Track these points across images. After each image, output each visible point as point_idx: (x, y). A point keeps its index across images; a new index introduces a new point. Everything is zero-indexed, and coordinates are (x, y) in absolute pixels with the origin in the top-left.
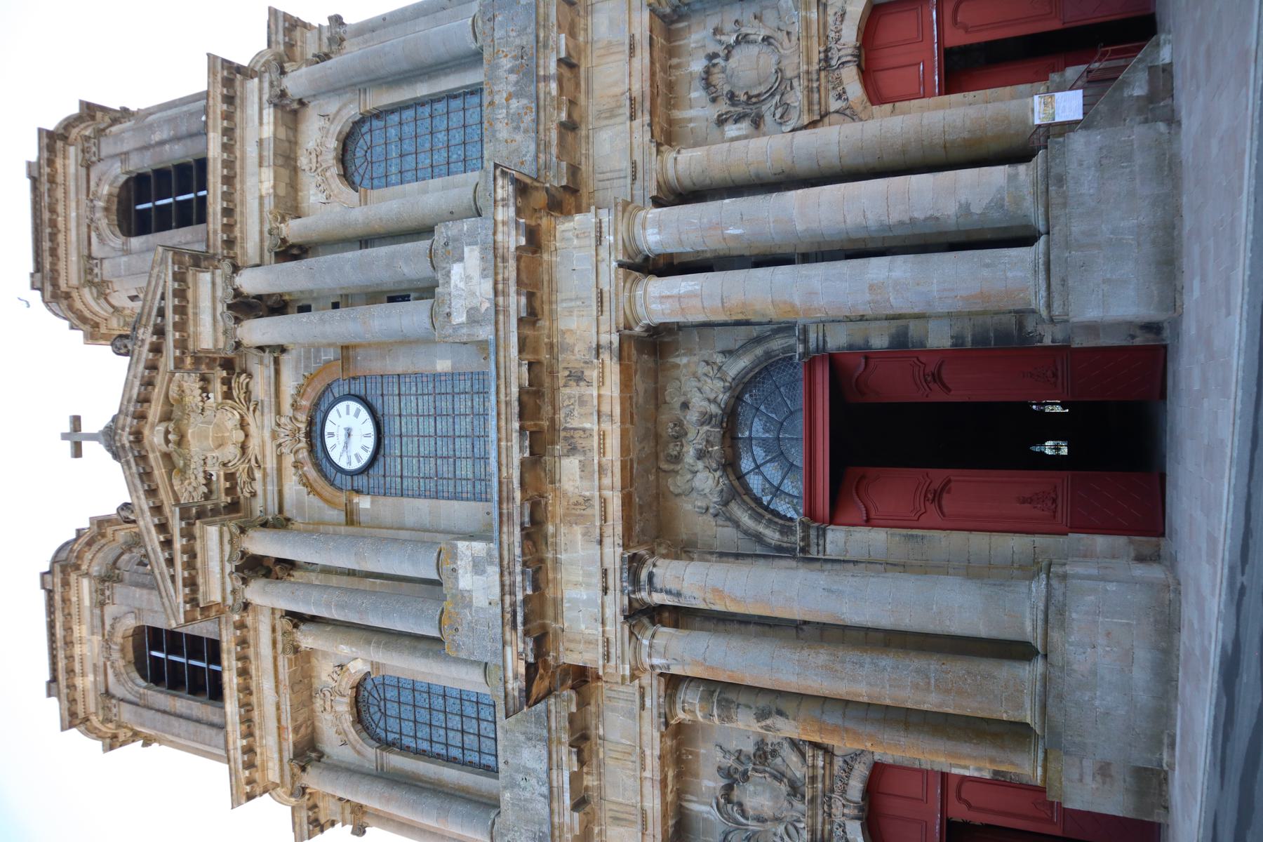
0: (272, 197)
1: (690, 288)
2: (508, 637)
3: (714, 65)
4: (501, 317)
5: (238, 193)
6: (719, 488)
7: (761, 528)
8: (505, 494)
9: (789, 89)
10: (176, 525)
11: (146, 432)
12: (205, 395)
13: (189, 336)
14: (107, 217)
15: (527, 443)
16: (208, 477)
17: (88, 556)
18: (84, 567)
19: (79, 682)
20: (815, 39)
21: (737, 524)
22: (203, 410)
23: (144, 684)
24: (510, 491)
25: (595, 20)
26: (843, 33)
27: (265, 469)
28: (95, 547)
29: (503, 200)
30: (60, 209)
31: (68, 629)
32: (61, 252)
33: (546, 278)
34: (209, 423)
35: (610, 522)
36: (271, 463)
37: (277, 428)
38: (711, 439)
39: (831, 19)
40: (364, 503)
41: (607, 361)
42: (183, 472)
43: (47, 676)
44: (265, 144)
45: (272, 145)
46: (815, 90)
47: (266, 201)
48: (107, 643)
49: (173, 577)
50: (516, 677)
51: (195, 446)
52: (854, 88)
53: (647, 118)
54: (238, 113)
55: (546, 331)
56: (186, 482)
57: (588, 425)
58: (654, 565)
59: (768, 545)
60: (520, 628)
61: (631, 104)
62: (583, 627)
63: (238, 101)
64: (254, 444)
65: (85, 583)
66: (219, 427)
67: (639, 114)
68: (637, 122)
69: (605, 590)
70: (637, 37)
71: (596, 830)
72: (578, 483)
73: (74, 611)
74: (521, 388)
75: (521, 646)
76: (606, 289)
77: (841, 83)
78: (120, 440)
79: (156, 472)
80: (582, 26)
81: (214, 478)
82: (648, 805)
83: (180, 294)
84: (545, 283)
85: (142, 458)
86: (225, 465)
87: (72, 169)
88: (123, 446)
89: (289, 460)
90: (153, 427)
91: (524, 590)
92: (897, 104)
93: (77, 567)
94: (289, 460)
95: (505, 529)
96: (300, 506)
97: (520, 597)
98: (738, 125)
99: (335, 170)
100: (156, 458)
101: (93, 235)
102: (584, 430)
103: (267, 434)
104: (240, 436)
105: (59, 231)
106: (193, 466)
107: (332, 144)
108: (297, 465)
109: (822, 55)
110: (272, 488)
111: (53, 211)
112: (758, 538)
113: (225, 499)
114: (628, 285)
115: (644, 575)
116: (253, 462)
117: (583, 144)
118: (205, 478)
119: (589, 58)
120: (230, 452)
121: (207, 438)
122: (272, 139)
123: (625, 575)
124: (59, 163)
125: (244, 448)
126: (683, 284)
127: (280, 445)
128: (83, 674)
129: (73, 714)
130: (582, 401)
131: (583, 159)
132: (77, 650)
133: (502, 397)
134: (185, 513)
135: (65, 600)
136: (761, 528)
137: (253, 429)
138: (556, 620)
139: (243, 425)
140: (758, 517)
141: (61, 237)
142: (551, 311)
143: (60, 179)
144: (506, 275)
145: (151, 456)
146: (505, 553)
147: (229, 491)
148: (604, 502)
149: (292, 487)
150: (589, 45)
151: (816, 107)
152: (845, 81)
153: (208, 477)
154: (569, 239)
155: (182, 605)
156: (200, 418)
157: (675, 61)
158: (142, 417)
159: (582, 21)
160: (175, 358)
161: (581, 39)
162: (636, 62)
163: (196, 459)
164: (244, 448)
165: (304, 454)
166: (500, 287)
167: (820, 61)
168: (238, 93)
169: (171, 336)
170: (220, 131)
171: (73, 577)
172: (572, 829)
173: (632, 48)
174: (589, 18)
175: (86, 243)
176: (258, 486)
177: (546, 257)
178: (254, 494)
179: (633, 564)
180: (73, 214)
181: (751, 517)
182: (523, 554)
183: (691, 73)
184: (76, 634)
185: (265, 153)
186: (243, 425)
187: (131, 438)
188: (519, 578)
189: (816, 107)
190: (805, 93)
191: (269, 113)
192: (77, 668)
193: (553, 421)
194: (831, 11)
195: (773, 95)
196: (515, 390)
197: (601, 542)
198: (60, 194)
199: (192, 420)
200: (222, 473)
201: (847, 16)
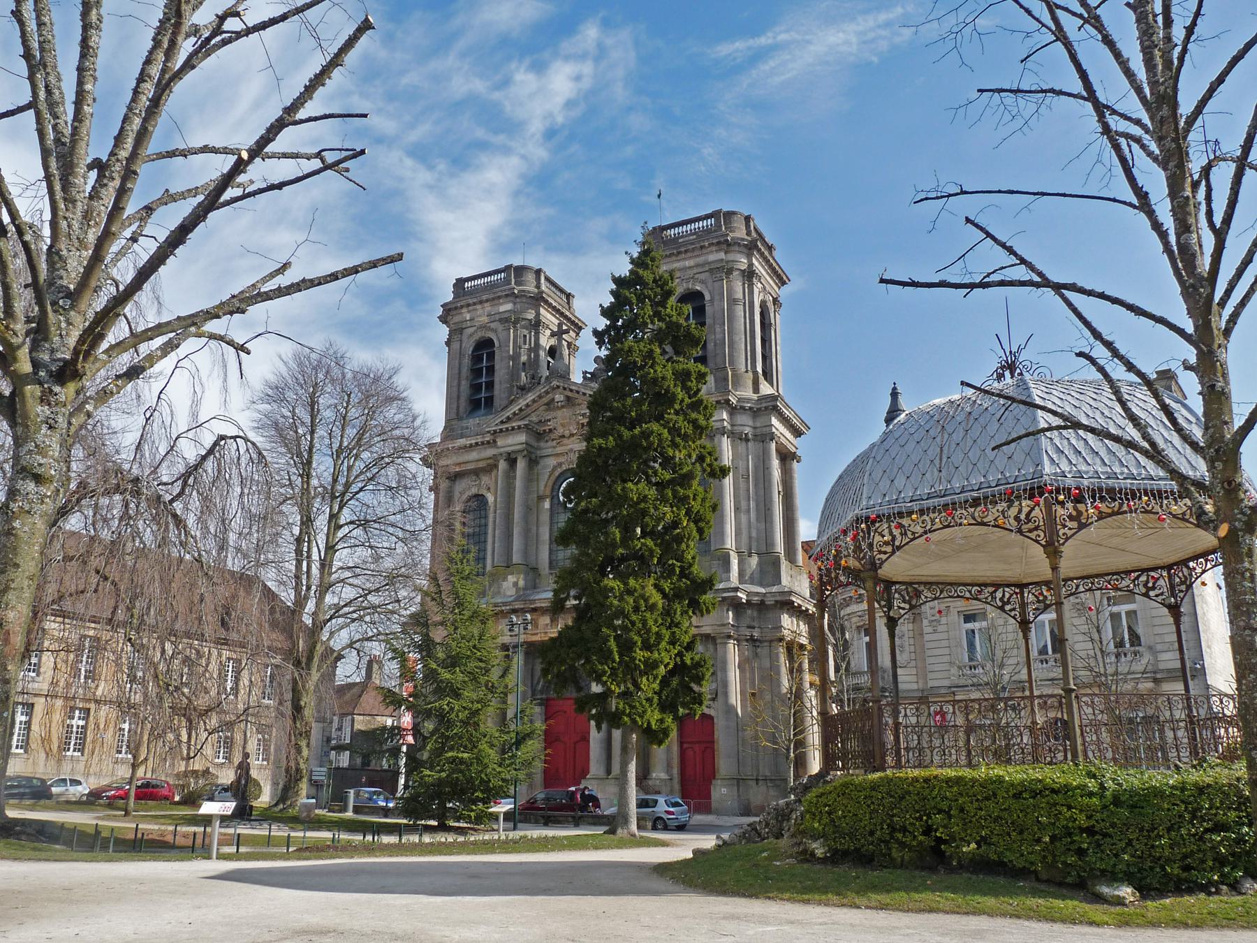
16: (549, 420)
18: (518, 300)
19: (464, 310)
30: (689, 254)
31: (487, 301)
36: (559, 450)
40: (547, 505)
42: (547, 410)
48: (483, 327)
49: (502, 422)
51: (559, 413)
64: (565, 441)
66: (569, 424)
73: (496, 302)
85: (547, 393)
89: (561, 459)
94: (561, 459)
96: (545, 467)
104: (567, 433)
108: (560, 465)
110: (550, 451)
111: (686, 251)
113: (541, 429)
120: (560, 431)
124: (714, 248)
125: (563, 436)
128: (469, 312)
129: (450, 310)
132: (478, 307)
135: (499, 297)
137: (572, 439)
139: (572, 435)
143: (704, 251)
147: (544, 431)
149: (552, 462)
153: (549, 420)
156: (571, 413)
164: (563, 436)
165: (564, 467)
176: (550, 444)
178: (547, 441)
180: (687, 263)
184: (486, 305)
186: (572, 435)
192: (471, 308)
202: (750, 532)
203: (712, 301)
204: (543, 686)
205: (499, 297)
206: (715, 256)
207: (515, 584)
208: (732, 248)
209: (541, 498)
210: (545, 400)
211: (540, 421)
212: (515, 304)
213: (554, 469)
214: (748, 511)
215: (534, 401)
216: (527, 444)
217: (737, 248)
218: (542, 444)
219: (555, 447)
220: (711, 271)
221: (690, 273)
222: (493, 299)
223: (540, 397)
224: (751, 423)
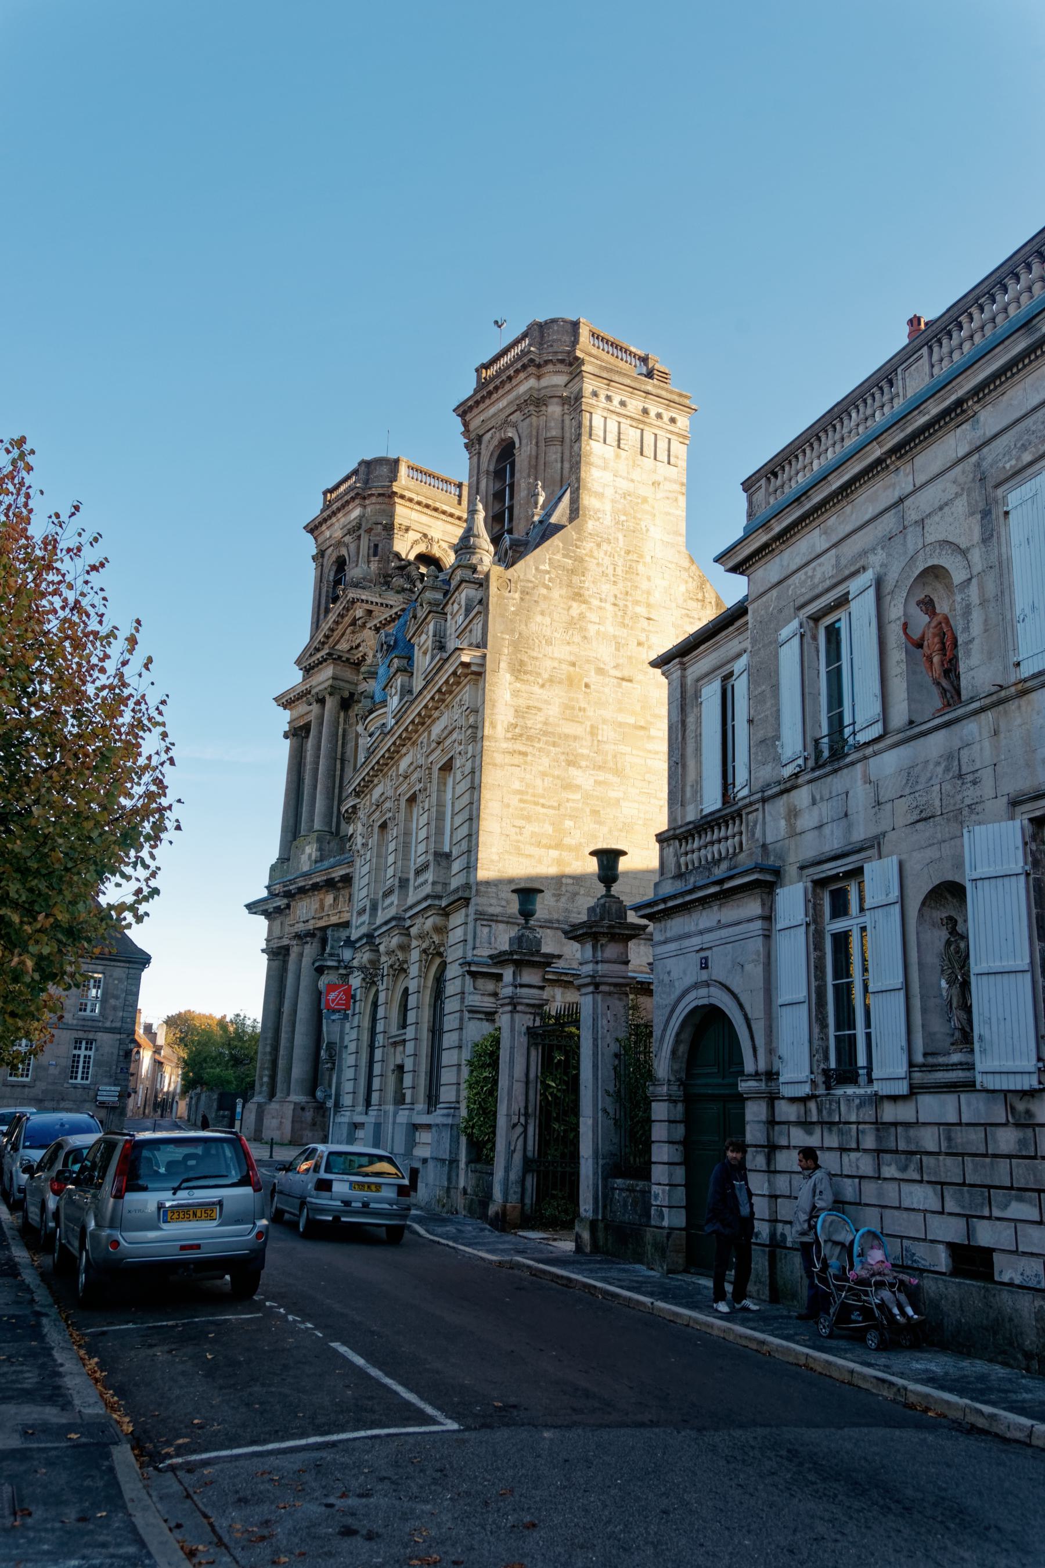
10: (323, 653)
16: (358, 646)
17: (374, 499)
18: (367, 502)
19: (324, 527)
23: (331, 578)
24: (310, 879)
28: (380, 500)
30: (501, 392)
31: (339, 510)
32: (482, 406)
42: (353, 632)
43: (330, 486)
48: (339, 543)
49: (311, 655)
65: (357, 513)
87: (522, 389)
93: (364, 498)
97: (291, 887)
101: (489, 435)
111: (496, 388)
124: (522, 375)
132: (334, 520)
135: (347, 503)
141: (488, 402)
143: (514, 382)
148: (322, 918)
153: (358, 646)
171: (357, 501)
175: (487, 428)
184: (340, 515)
192: (329, 523)
198: (508, 387)
205: (347, 503)
206: (526, 385)
208: (545, 370)
210: (347, 620)
211: (352, 648)
212: (365, 507)
215: (337, 623)
216: (333, 678)
217: (550, 367)
220: (519, 408)
221: (503, 416)
222: (343, 506)
223: (341, 616)
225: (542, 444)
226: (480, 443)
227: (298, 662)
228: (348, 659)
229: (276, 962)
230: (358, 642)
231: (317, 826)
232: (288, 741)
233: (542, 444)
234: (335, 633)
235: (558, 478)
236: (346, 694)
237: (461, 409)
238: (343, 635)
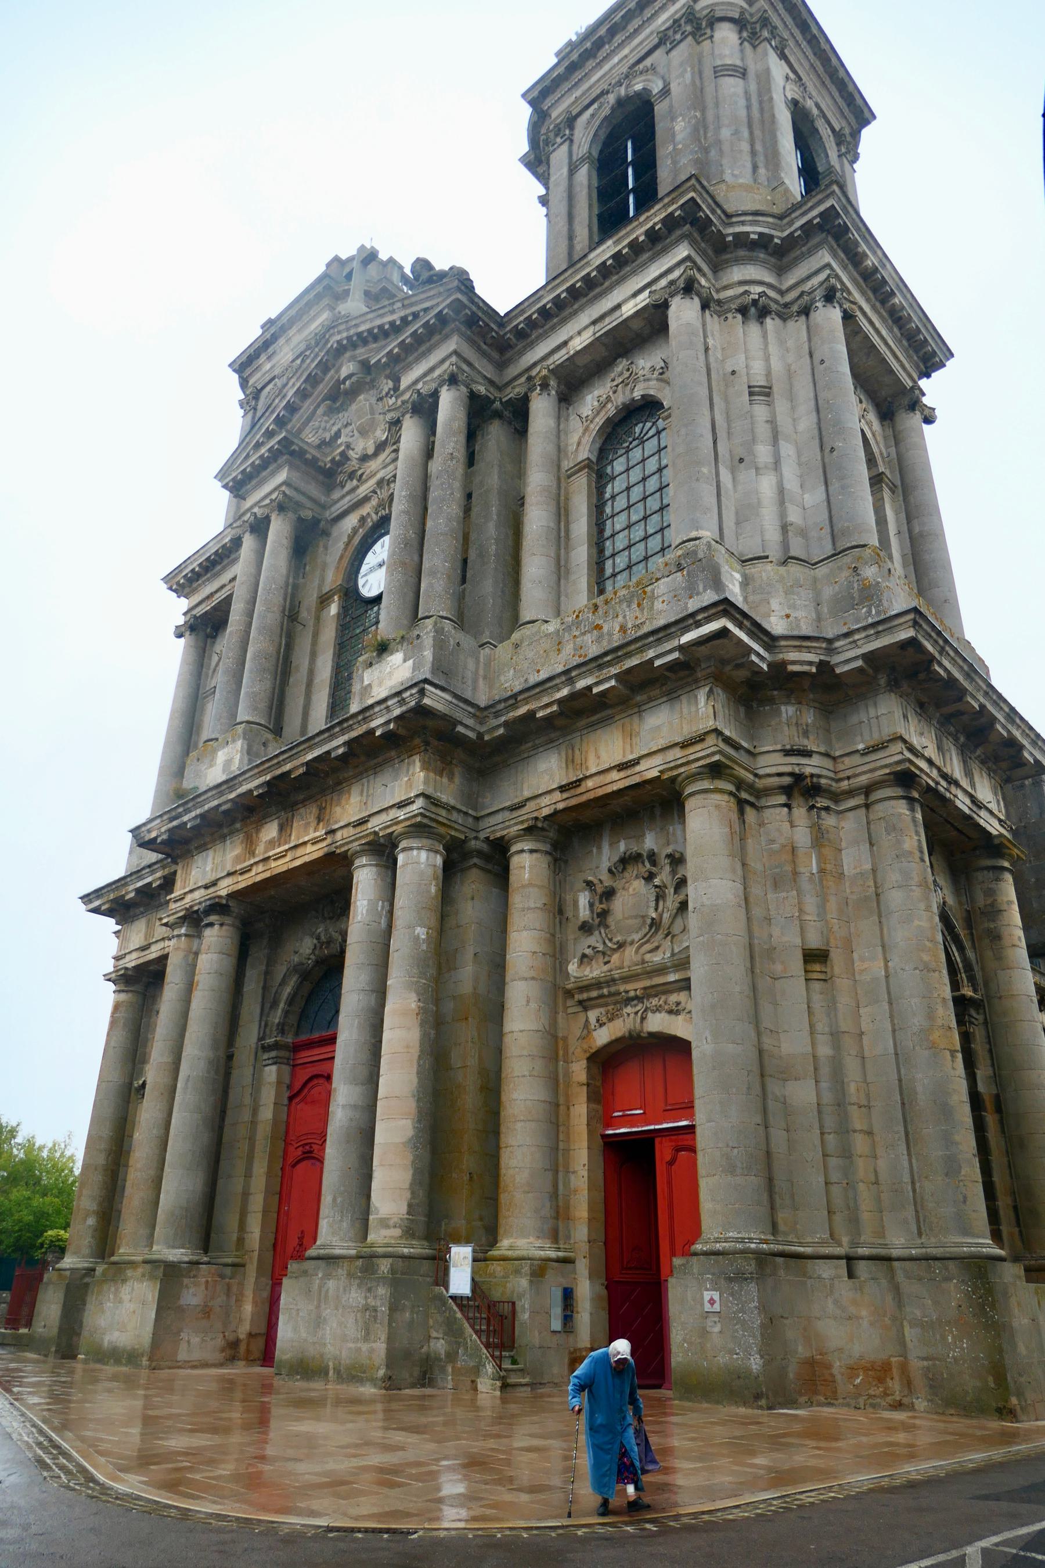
0: (566, 357)
1: (360, 910)
2: (165, 817)
3: (643, 863)
4: (326, 735)
5: (571, 310)
6: (305, 961)
7: (282, 1005)
8: (231, 784)
9: (606, 959)
11: (348, 354)
12: (392, 392)
13: (404, 360)
14: (613, 109)
15: (261, 791)
16: (338, 434)
19: (263, 358)
20: (647, 983)
21: (283, 983)
22: (381, 399)
25: (663, 706)
26: (658, 1014)
27: (357, 487)
29: (403, 699)
30: (618, 38)
33: (380, 759)
34: (372, 413)
35: (240, 878)
36: (363, 490)
37: (385, 483)
38: (332, 945)
39: (673, 998)
40: (334, 609)
41: (324, 844)
42: (331, 411)
44: (617, 313)
45: (614, 324)
46: (600, 992)
47: (563, 351)
49: (247, 456)
50: (149, 831)
52: (602, 1037)
53: (561, 806)
54: (646, 256)
55: (346, 775)
56: (326, 418)
57: (293, 838)
58: (222, 925)
59: (268, 1016)
60: (171, 825)
61: (572, 783)
62: (193, 873)
63: (659, 247)
67: (565, 795)
68: (557, 796)
69: (206, 887)
70: (638, 768)
71: (142, 909)
72: (264, 840)
74: (289, 772)
75: (163, 830)
76: (370, 825)
77: (610, 1020)
78: (330, 336)
79: (321, 386)
80: (652, 694)
81: (339, 441)
82: (154, 948)
83: (430, 331)
84: (375, 761)
86: (348, 446)
88: (327, 341)
90: (353, 358)
91: (190, 820)
92: (585, 1088)
95: (214, 792)
98: (587, 906)
99: (611, 410)
100: (332, 378)
101: (595, 106)
102: (290, 835)
103: (379, 476)
104: (371, 451)
105: (595, 57)
106: (340, 415)
107: (637, 394)
108: (363, 520)
109: (632, 994)
112: (275, 1004)
114: (366, 847)
115: (213, 918)
116: (360, 472)
117: (542, 739)
118: (336, 434)
119: (623, 715)
121: (360, 418)
122: (621, 320)
123: (208, 903)
126: (365, 902)
127: (376, 493)
130: (308, 824)
131: (530, 744)
133: (281, 758)
134: (285, 442)
136: (282, 1005)
137: (382, 457)
138: (196, 848)
140: (291, 1001)
141: (591, 64)
142: (361, 773)
144: (355, 727)
145: (332, 372)
146: (203, 798)
150: (636, 710)
151: (585, 996)
152: (611, 1024)
153: (338, 434)
154: (408, 771)
155: (231, 477)
156: (373, 400)
157: (658, 812)
158: (354, 346)
159: (658, 691)
160: (379, 360)
161: (639, 698)
162: (615, 775)
163: (346, 414)
164: (365, 458)
166: (345, 725)
167: (627, 992)
168: (668, 240)
169: (392, 345)
170: (617, 249)
171: (326, 301)
172: (127, 893)
173: (622, 767)
174: (665, 699)
177: (393, 753)
179: (217, 907)
181: (289, 994)
182: (207, 811)
183: (644, 835)
185: (607, 320)
187: (335, 345)
188: (193, 814)
189: (585, 996)
190: (593, 981)
191: (643, 300)
193: (296, 803)
194: (682, 997)
195: (604, 943)
196: (287, 767)
197: (229, 874)
199: (371, 392)
200: (343, 448)
201: (673, 1017)
202: (783, 514)
203: (666, 92)
204: (286, 1013)
207: (228, 763)
209: (324, 601)
210: (323, 388)
213: (355, 531)
214: (777, 464)
218: (336, 495)
219: (354, 489)
224: (769, 278)
225: (708, 72)
226: (572, 128)
227: (221, 475)
228: (315, 460)
229: (130, 995)
230: (335, 429)
231: (243, 715)
232: (182, 640)
233: (708, 72)
234: (297, 416)
235: (743, 113)
236: (307, 514)
237: (535, 93)
238: (309, 420)
